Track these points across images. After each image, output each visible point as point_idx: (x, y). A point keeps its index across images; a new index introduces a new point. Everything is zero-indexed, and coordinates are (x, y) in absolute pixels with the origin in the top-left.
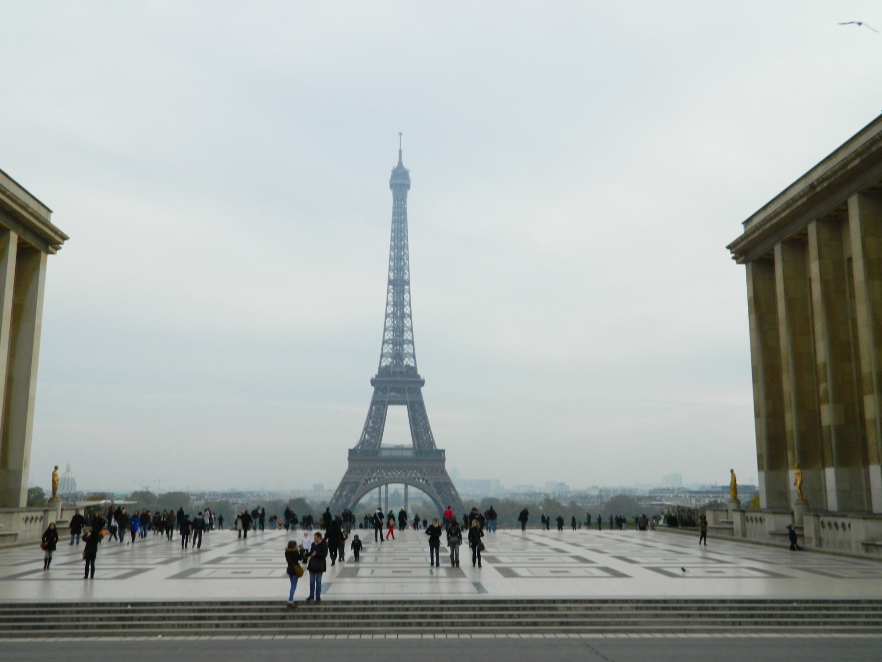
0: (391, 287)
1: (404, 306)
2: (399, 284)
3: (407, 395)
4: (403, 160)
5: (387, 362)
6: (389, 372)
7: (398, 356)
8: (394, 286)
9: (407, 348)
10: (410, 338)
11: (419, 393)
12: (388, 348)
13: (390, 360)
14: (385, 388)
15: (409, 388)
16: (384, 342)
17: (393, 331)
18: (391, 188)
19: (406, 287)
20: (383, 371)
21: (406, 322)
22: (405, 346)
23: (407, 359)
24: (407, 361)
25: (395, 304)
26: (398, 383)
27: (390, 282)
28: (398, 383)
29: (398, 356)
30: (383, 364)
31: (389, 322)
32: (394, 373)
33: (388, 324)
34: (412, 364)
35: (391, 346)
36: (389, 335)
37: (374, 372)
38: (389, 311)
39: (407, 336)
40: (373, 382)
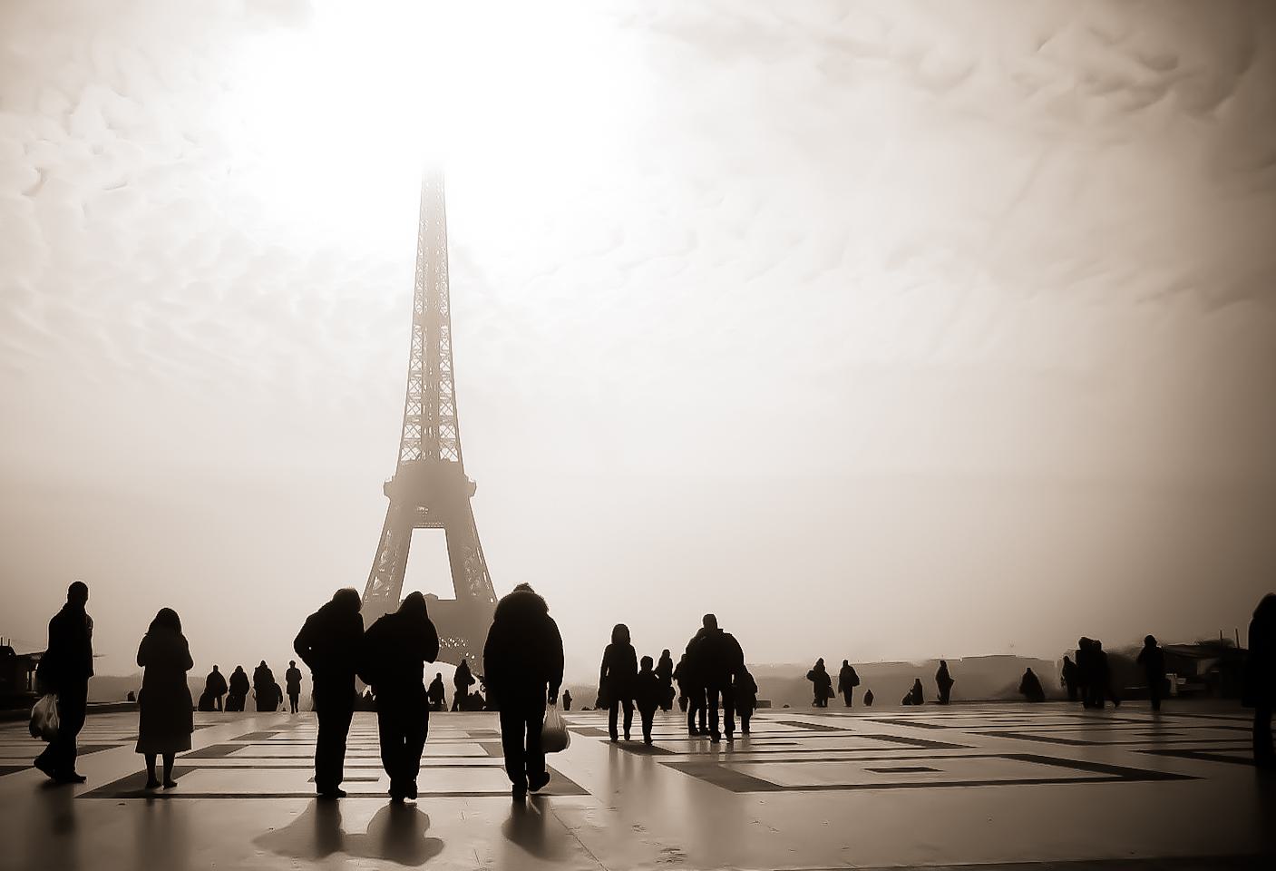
0: (418, 327)
1: (440, 360)
2: (432, 322)
5: (411, 454)
7: (430, 442)
9: (446, 432)
10: (450, 413)
12: (414, 432)
13: (416, 451)
16: (407, 420)
19: (446, 327)
21: (443, 387)
22: (442, 428)
23: (445, 451)
24: (447, 454)
26: (432, 492)
28: (432, 492)
29: (430, 442)
30: (405, 459)
31: (416, 388)
33: (414, 391)
34: (454, 459)
35: (418, 428)
36: (415, 410)
37: (390, 472)
38: (416, 369)
39: (446, 410)
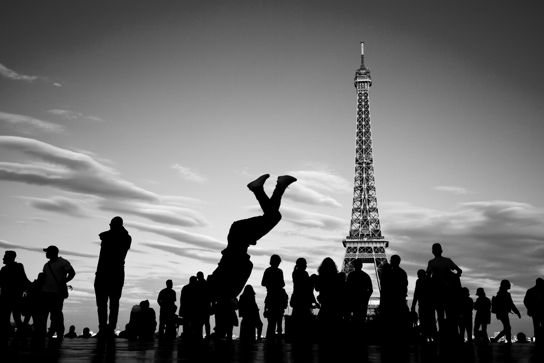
3: (374, 253)
4: (365, 64)
6: (358, 235)
8: (359, 164)
11: (384, 252)
13: (358, 225)
14: (355, 248)
15: (375, 248)
16: (354, 210)
17: (361, 201)
18: (356, 86)
20: (353, 234)
25: (362, 180)
27: (357, 161)
30: (353, 228)
32: (363, 235)
40: (344, 243)
